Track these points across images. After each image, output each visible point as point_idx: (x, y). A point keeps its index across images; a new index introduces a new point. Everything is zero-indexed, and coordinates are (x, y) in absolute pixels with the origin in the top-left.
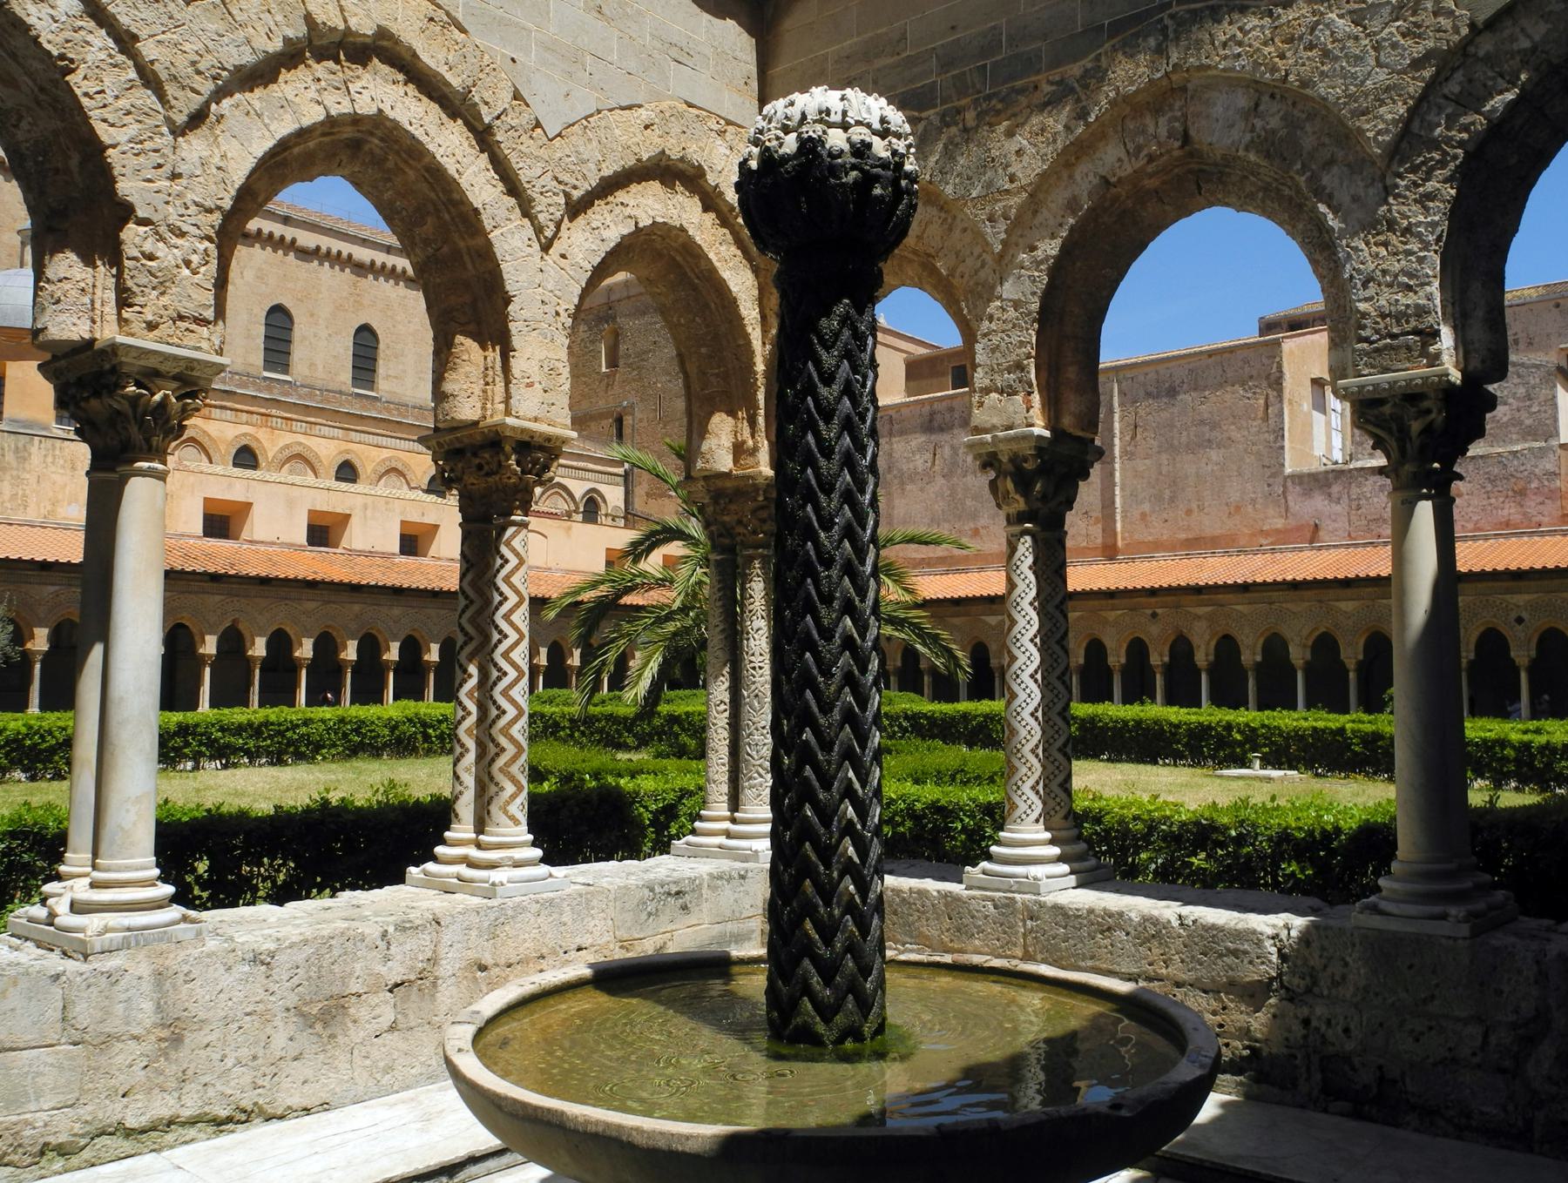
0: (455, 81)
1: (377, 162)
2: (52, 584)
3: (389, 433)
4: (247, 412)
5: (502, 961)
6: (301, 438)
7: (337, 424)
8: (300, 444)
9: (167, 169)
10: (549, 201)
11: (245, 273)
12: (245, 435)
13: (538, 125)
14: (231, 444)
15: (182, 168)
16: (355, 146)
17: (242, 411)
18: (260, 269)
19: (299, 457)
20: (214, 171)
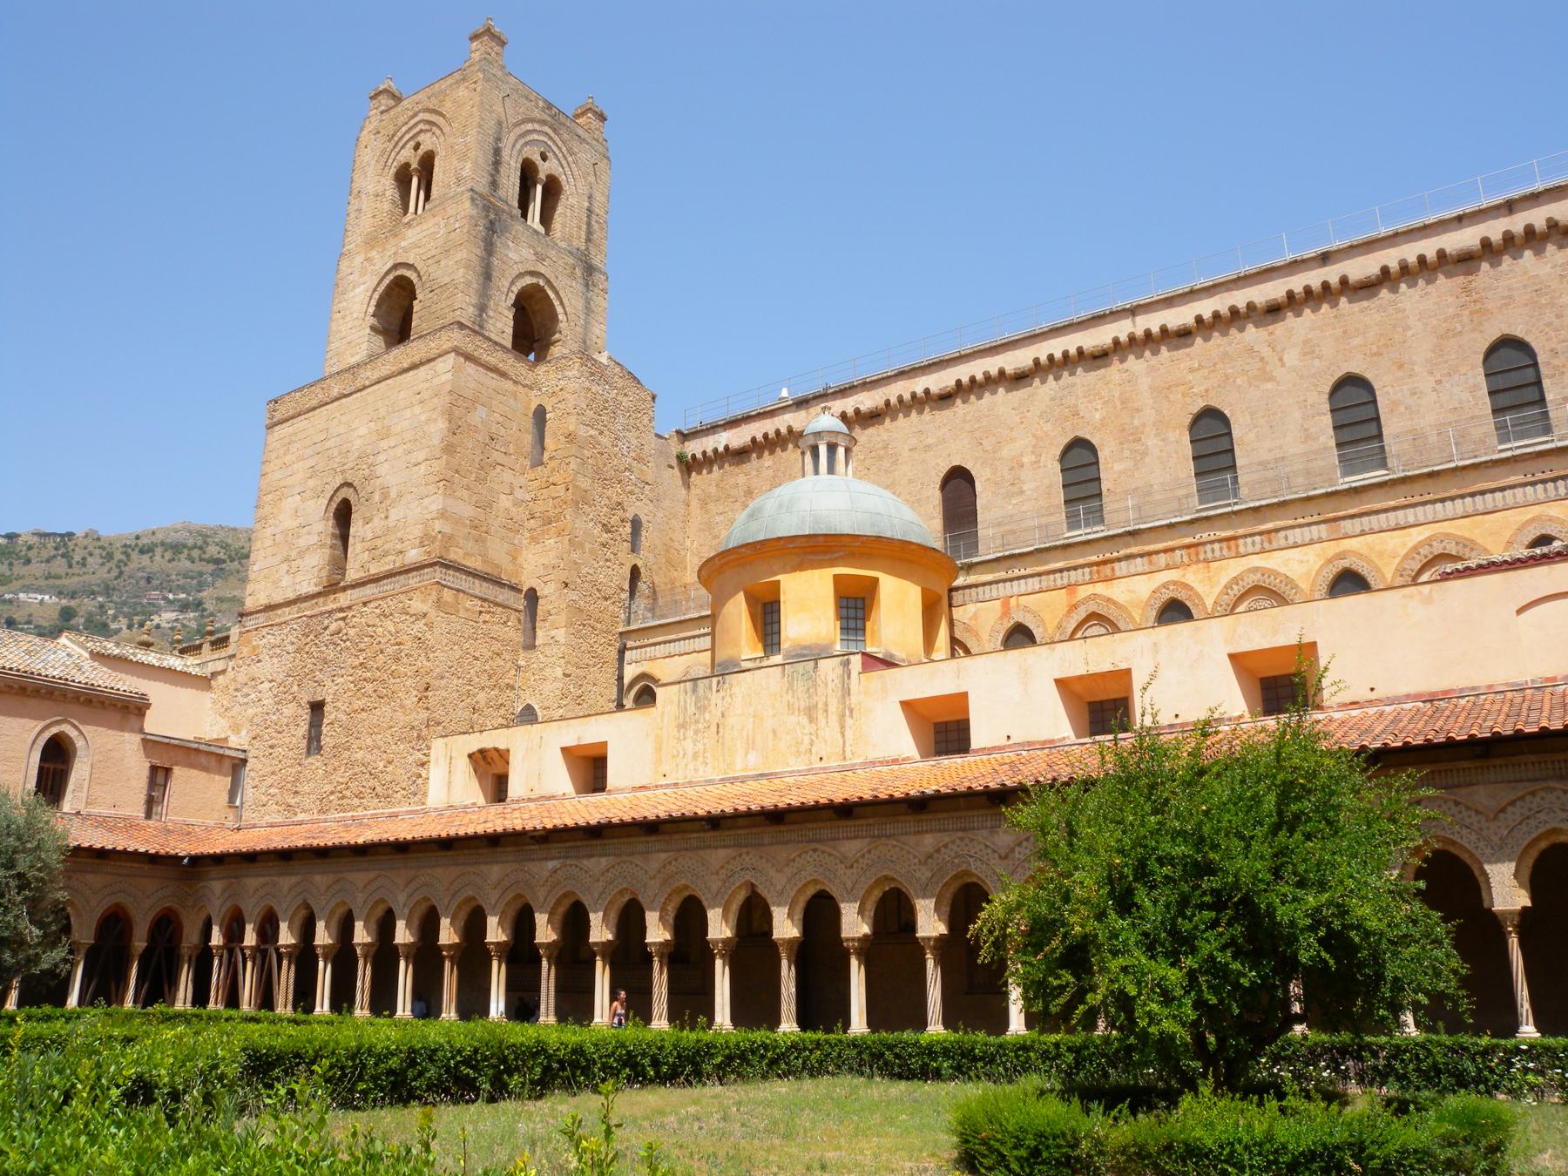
2: (553, 858)
3: (1417, 499)
4: (1165, 551)
6: (1256, 561)
7: (1316, 518)
8: (1255, 570)
11: (1285, 358)
12: (1165, 586)
14: (1148, 604)
17: (1157, 552)
18: (1306, 342)
19: (1256, 589)
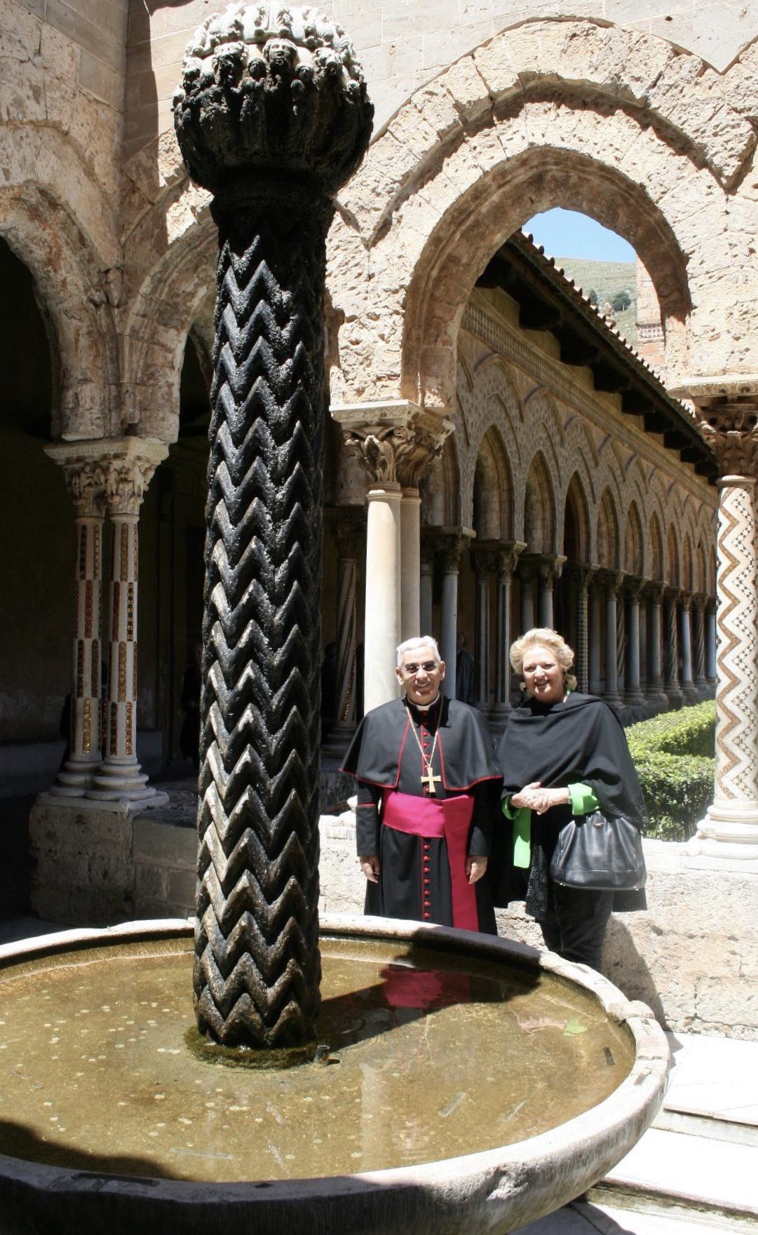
0: (599, 78)
1: (562, 184)
5: (681, 930)
9: (365, 276)
10: (726, 138)
13: (706, 66)
15: (374, 270)
16: (538, 182)
20: (396, 260)
